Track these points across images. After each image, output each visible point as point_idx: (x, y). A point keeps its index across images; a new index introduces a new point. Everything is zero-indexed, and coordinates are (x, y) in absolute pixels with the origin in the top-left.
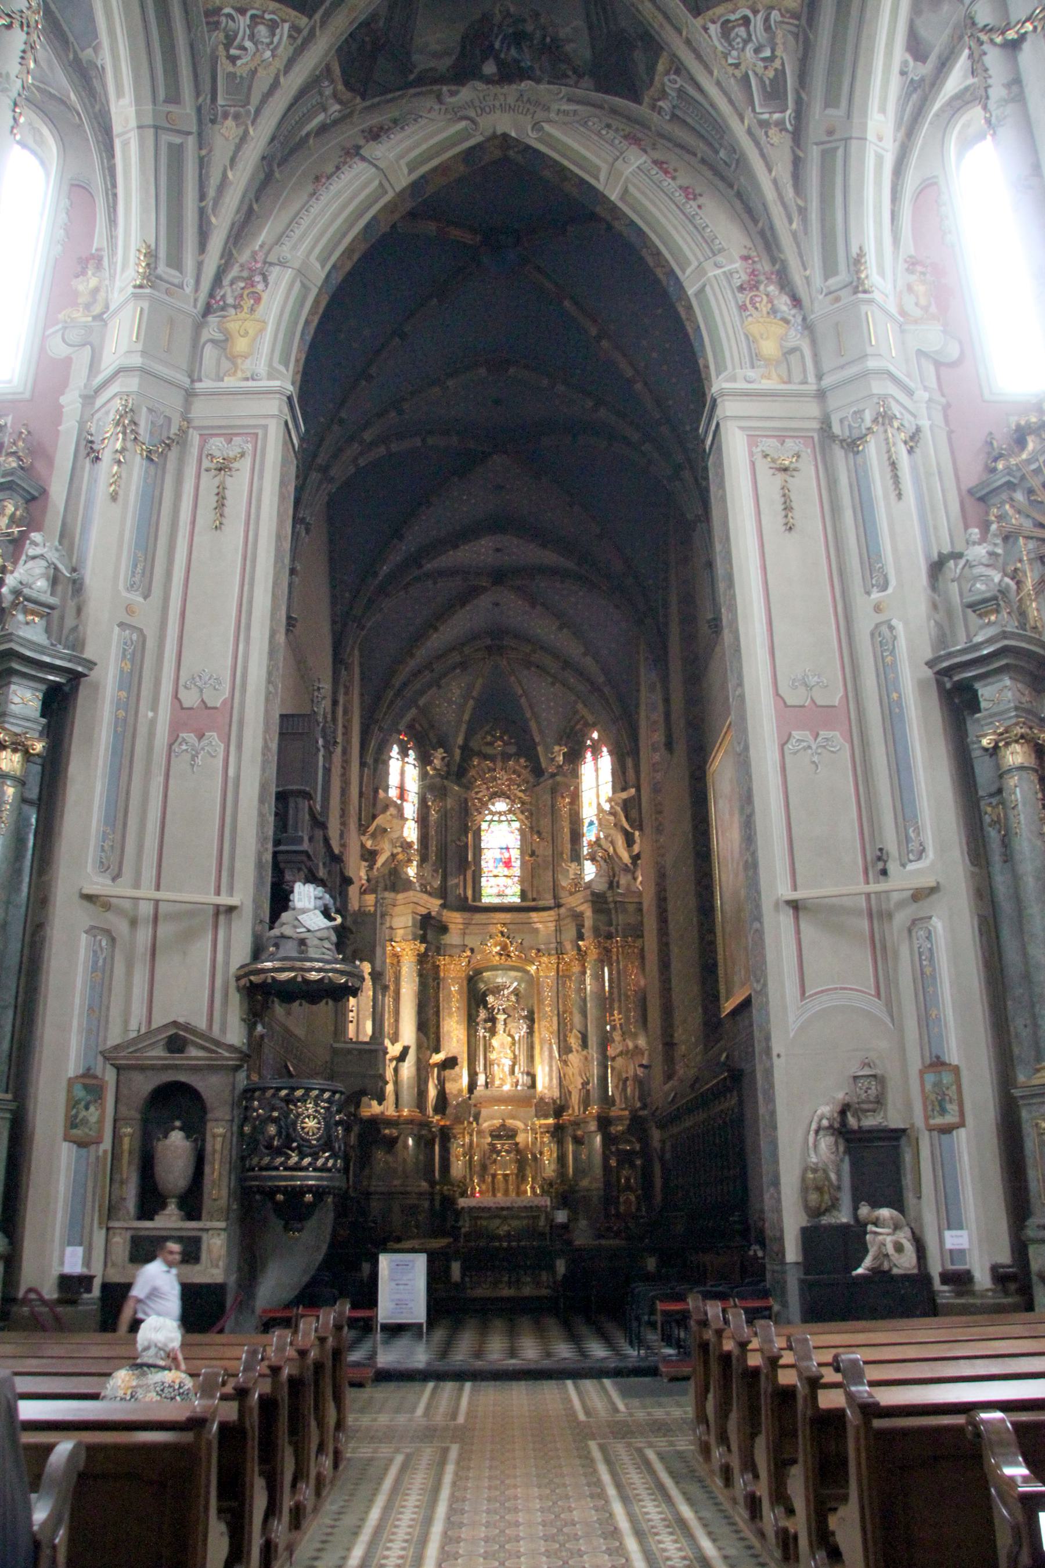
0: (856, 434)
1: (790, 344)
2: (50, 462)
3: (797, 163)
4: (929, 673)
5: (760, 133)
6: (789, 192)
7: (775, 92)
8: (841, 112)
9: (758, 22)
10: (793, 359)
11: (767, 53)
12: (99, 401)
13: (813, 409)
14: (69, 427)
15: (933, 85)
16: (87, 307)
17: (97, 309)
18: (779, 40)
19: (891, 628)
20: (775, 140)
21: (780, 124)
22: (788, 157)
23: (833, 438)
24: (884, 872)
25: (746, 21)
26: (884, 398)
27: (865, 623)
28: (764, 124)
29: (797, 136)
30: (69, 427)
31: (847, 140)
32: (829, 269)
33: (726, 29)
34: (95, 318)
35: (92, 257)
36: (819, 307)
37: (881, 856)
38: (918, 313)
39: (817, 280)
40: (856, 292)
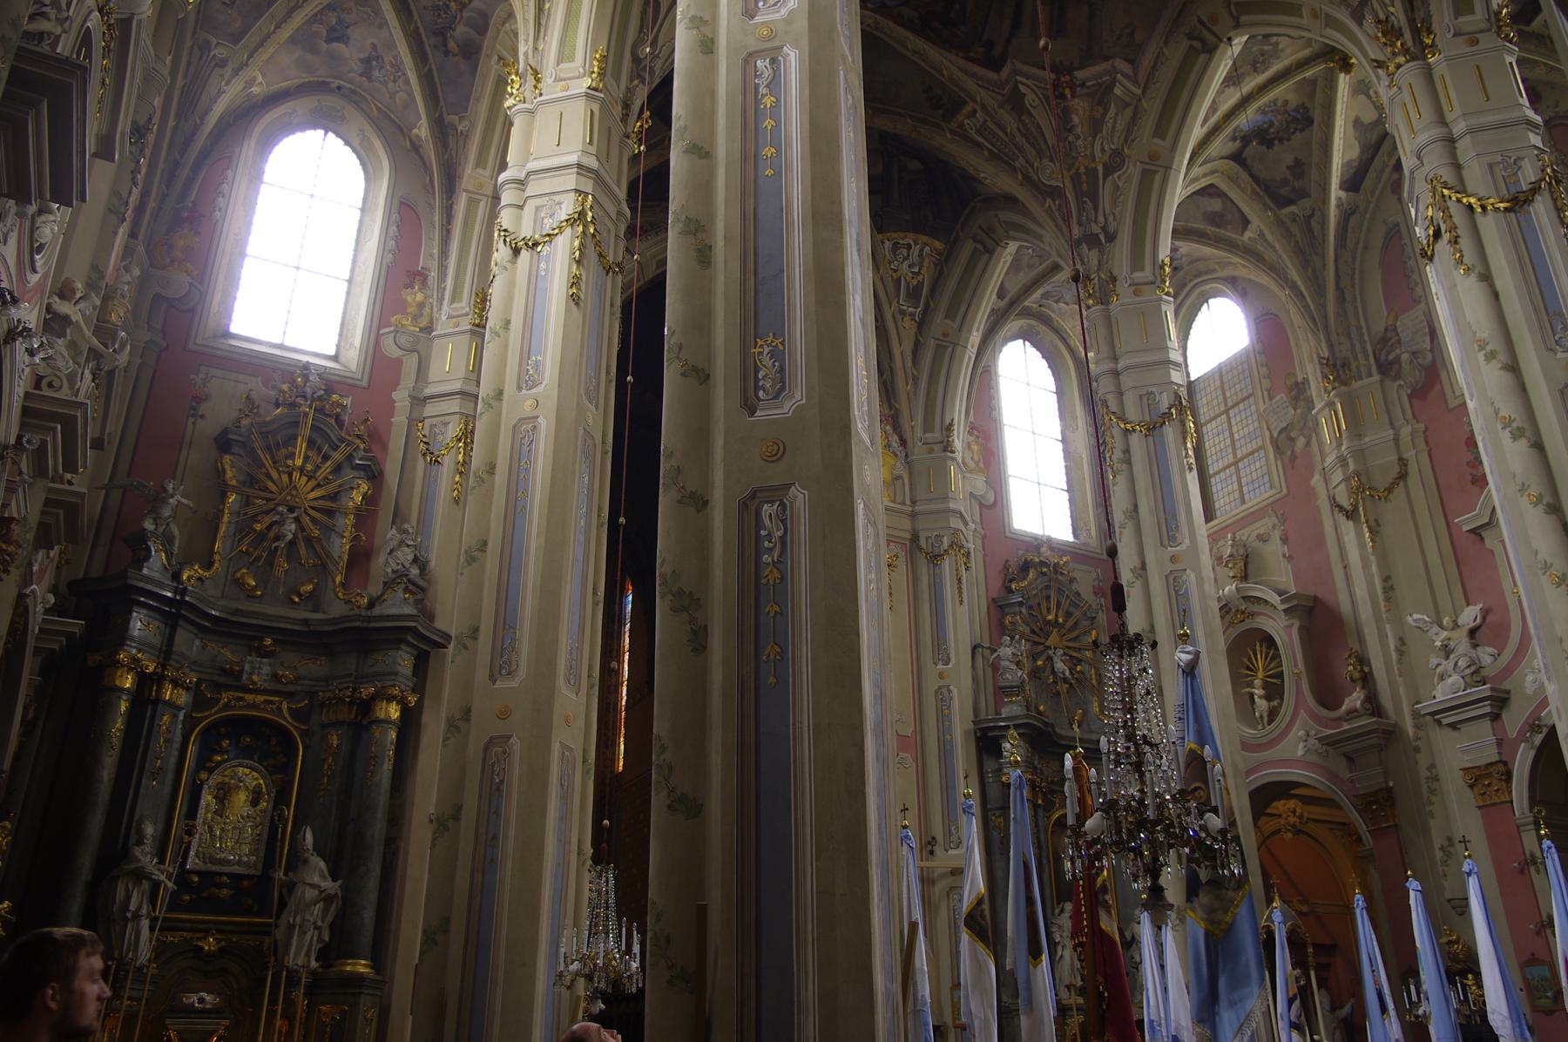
0: (936, 551)
1: (897, 473)
2: (384, 448)
3: (917, 344)
4: (971, 726)
5: (899, 317)
6: (910, 364)
7: (914, 295)
8: (956, 325)
9: (916, 250)
10: (898, 483)
11: (916, 270)
12: (430, 409)
13: (906, 524)
14: (400, 419)
15: (1004, 315)
16: (415, 318)
17: (424, 322)
18: (926, 263)
19: (950, 691)
20: (907, 325)
21: (912, 315)
22: (912, 338)
23: (920, 549)
24: (932, 853)
25: (909, 247)
26: (956, 531)
27: (931, 685)
28: (902, 312)
29: (921, 326)
31: (955, 345)
32: (928, 427)
33: (895, 247)
34: (421, 330)
35: (419, 274)
36: (918, 452)
37: (932, 841)
38: (972, 465)
39: (919, 432)
40: (945, 450)
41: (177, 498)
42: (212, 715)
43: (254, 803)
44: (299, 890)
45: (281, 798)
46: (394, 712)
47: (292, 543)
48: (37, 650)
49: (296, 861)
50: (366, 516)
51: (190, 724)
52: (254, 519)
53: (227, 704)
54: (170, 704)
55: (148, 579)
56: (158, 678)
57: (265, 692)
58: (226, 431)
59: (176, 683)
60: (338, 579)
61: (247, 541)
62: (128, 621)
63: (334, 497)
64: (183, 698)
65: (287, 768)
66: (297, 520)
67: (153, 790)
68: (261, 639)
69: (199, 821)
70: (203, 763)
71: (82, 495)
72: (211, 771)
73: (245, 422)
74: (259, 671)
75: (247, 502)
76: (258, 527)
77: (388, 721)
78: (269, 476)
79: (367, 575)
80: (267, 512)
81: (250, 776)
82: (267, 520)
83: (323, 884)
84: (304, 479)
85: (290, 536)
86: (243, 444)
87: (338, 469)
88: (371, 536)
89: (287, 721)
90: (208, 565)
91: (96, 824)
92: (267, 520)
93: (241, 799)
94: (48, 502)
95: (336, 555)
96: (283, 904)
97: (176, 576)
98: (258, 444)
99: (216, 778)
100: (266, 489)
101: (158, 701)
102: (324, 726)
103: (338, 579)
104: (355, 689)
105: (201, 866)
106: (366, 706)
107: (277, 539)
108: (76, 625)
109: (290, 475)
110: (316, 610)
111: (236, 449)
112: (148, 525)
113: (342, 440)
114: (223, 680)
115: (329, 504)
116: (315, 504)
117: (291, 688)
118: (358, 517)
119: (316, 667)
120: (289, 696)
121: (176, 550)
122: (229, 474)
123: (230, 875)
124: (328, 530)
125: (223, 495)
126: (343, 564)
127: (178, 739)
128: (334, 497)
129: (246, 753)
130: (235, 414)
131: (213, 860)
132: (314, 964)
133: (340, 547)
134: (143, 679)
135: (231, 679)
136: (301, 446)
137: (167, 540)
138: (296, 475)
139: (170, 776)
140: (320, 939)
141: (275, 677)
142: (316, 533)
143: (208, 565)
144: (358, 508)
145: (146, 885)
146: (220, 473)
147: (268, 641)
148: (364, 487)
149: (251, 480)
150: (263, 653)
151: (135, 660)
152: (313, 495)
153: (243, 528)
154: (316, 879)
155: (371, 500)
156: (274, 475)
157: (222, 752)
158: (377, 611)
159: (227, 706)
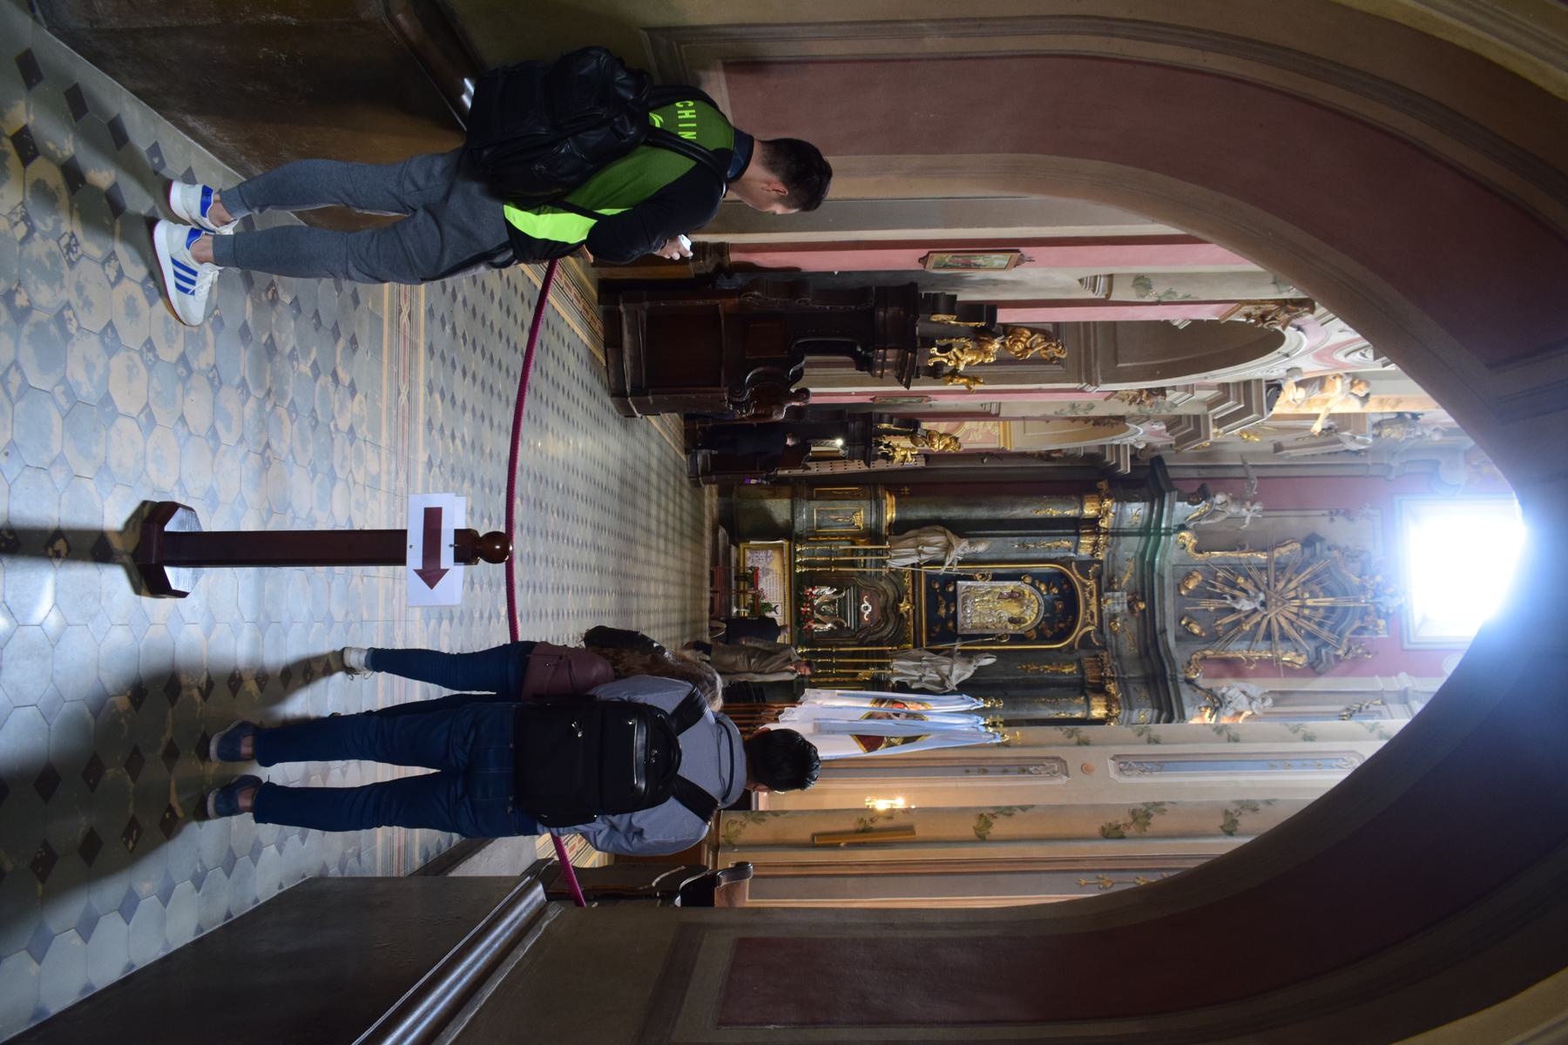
14: (1379, 683)
30: (1379, 683)
41: (1249, 513)
42: (1075, 576)
43: (1012, 620)
44: (947, 660)
45: (1016, 639)
46: (1098, 712)
47: (1233, 610)
48: (1103, 447)
49: (968, 655)
50: (1271, 667)
51: (1066, 562)
52: (1247, 577)
53: (1086, 587)
54: (1077, 546)
55: (1172, 508)
56: (1096, 531)
57: (1100, 611)
58: (1321, 540)
59: (1095, 544)
60: (1208, 653)
61: (1228, 575)
62: (1137, 500)
63: (1284, 638)
64: (1084, 552)
65: (1041, 638)
66: (1255, 611)
67: (1010, 546)
68: (1143, 600)
69: (994, 583)
70: (1037, 578)
71: (1207, 438)
72: (1032, 584)
73: (1335, 553)
74: (1116, 603)
75: (1262, 568)
76: (1241, 580)
77: (1089, 708)
78: (1290, 581)
79: (1218, 676)
80: (1256, 586)
81: (1031, 615)
82: (1249, 586)
83: (953, 678)
84: (1295, 610)
85: (1238, 607)
86: (1314, 555)
87: (1311, 636)
88: (1256, 674)
89: (1078, 632)
90: (1198, 550)
91: (981, 513)
92: (1249, 586)
93: (1014, 610)
94: (1197, 418)
95: (1233, 646)
96: (937, 652)
97: (1182, 527)
98: (1317, 567)
99: (1027, 589)
100: (1277, 580)
101: (1078, 534)
102: (1079, 661)
103: (1208, 653)
104: (1112, 679)
105: (960, 591)
106: (1100, 690)
107: (1234, 597)
108: (1126, 468)
109: (1296, 598)
110: (1178, 639)
111: (1307, 552)
112: (1220, 498)
113: (1340, 635)
114: (1104, 579)
115: (1277, 635)
116: (1274, 622)
117: (1106, 630)
118: (1270, 661)
119: (1128, 647)
120: (1100, 630)
121: (1203, 522)
122: (1283, 550)
123: (955, 613)
124: (1251, 636)
125: (1264, 550)
126: (1224, 654)
127: (1053, 556)
128: (1284, 638)
129: (1050, 607)
130: (1342, 544)
131: (965, 599)
132: (894, 680)
133: (1238, 650)
134: (1093, 522)
135: (1106, 583)
136: (1325, 602)
137: (1211, 514)
138: (1297, 602)
139: (1024, 556)
140: (913, 682)
141: (1114, 617)
142: (1247, 628)
143: (1198, 550)
144: (1278, 659)
145: (941, 556)
146: (1281, 544)
147: (1142, 606)
148: (1301, 661)
149: (1281, 568)
150: (1131, 605)
151: (1107, 512)
152: (1282, 620)
153: (1236, 569)
154: (956, 672)
155: (1290, 671)
156: (1292, 585)
157: (1048, 590)
158: (1184, 687)
159: (1084, 586)
